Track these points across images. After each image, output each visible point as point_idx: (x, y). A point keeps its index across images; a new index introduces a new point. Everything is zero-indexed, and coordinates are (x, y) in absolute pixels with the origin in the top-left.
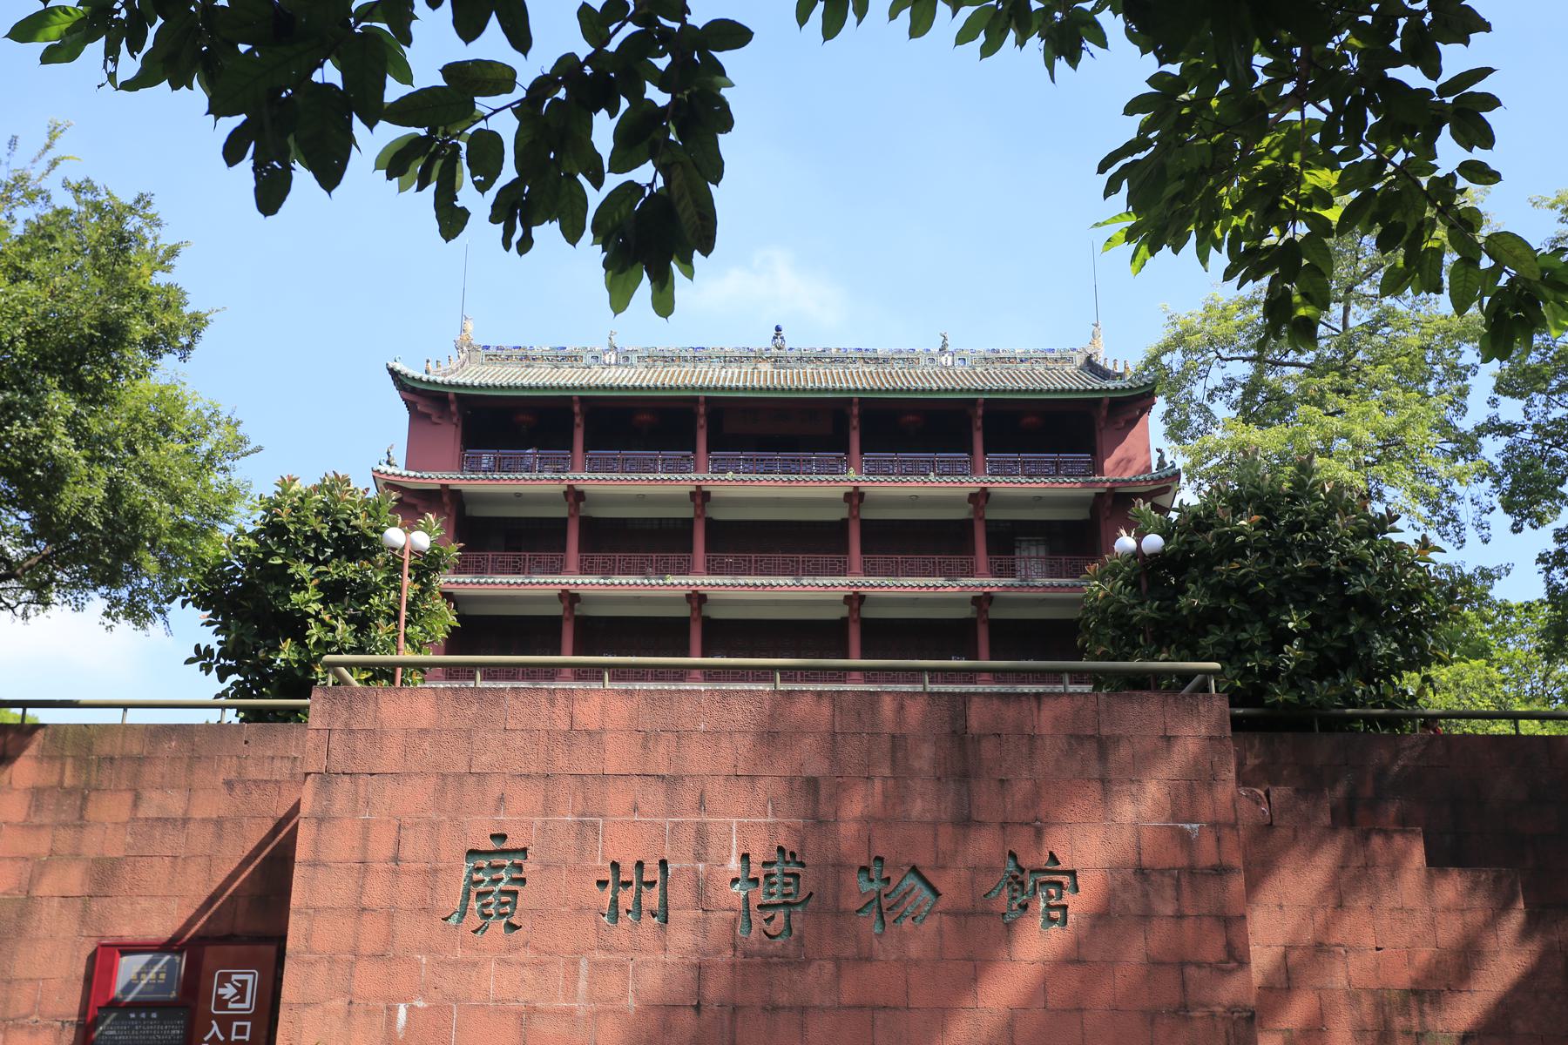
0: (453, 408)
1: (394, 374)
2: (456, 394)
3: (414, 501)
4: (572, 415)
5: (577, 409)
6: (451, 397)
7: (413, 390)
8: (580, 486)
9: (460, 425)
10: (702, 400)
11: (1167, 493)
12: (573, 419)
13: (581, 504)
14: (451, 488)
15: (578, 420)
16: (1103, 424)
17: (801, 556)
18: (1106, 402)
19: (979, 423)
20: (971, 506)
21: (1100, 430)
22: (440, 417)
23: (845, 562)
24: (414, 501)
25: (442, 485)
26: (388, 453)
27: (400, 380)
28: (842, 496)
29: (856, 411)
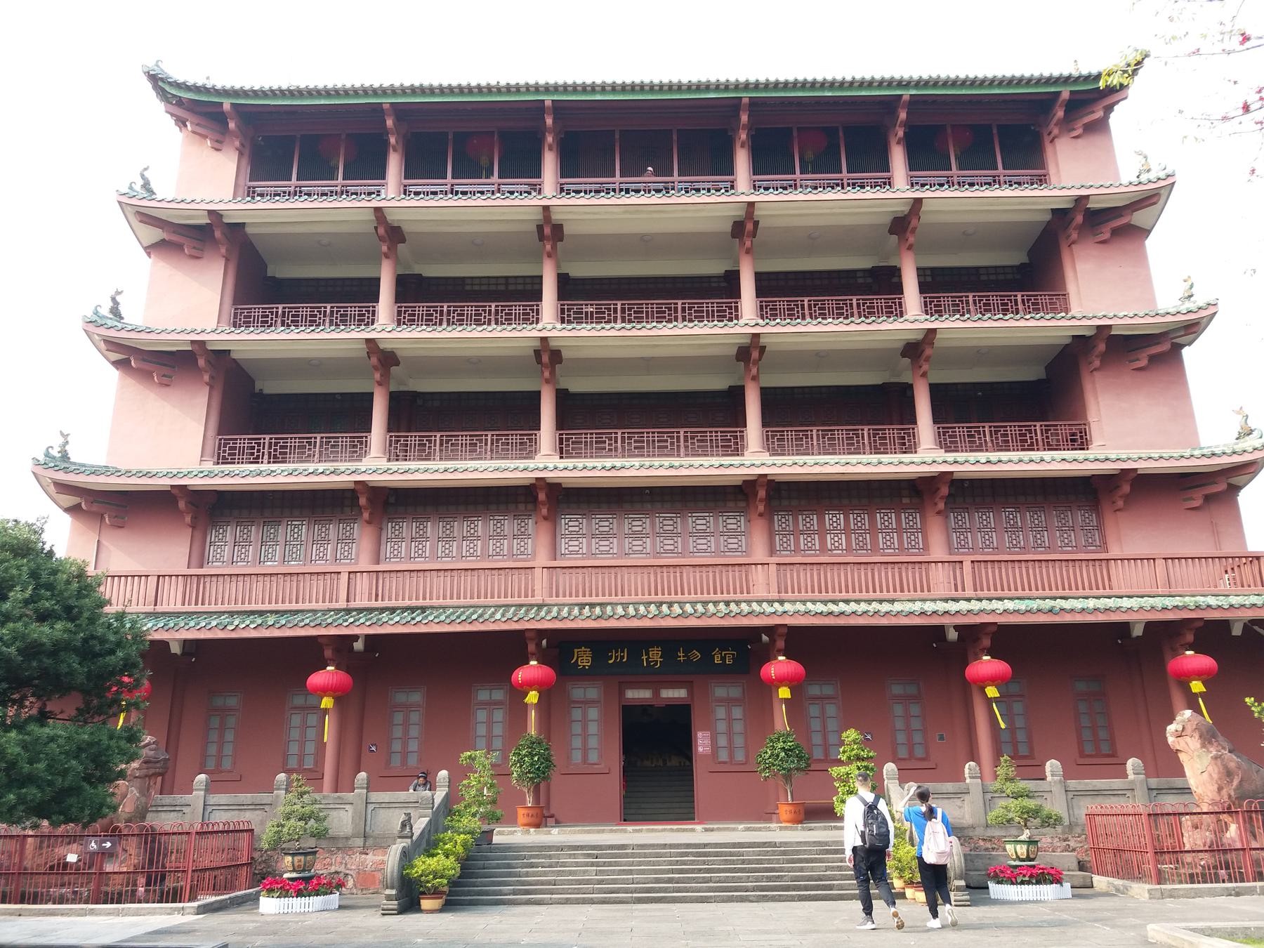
0: (232, 125)
1: (156, 80)
2: (232, 104)
3: (175, 238)
4: (385, 132)
5: (390, 123)
6: (227, 106)
7: (180, 102)
8: (392, 217)
9: (247, 152)
10: (548, 104)
11: (1155, 203)
12: (387, 142)
13: (400, 246)
14: (226, 220)
15: (392, 140)
16: (1056, 131)
17: (680, 302)
18: (1066, 95)
19: (901, 133)
20: (895, 238)
21: (1052, 141)
22: (217, 141)
23: (736, 308)
24: (175, 238)
25: (211, 213)
26: (142, 176)
27: (163, 90)
28: (728, 227)
29: (744, 118)
